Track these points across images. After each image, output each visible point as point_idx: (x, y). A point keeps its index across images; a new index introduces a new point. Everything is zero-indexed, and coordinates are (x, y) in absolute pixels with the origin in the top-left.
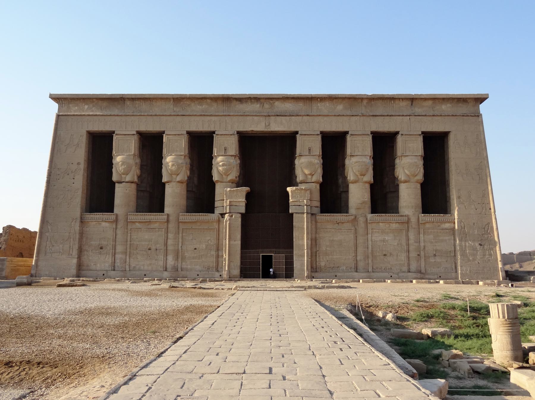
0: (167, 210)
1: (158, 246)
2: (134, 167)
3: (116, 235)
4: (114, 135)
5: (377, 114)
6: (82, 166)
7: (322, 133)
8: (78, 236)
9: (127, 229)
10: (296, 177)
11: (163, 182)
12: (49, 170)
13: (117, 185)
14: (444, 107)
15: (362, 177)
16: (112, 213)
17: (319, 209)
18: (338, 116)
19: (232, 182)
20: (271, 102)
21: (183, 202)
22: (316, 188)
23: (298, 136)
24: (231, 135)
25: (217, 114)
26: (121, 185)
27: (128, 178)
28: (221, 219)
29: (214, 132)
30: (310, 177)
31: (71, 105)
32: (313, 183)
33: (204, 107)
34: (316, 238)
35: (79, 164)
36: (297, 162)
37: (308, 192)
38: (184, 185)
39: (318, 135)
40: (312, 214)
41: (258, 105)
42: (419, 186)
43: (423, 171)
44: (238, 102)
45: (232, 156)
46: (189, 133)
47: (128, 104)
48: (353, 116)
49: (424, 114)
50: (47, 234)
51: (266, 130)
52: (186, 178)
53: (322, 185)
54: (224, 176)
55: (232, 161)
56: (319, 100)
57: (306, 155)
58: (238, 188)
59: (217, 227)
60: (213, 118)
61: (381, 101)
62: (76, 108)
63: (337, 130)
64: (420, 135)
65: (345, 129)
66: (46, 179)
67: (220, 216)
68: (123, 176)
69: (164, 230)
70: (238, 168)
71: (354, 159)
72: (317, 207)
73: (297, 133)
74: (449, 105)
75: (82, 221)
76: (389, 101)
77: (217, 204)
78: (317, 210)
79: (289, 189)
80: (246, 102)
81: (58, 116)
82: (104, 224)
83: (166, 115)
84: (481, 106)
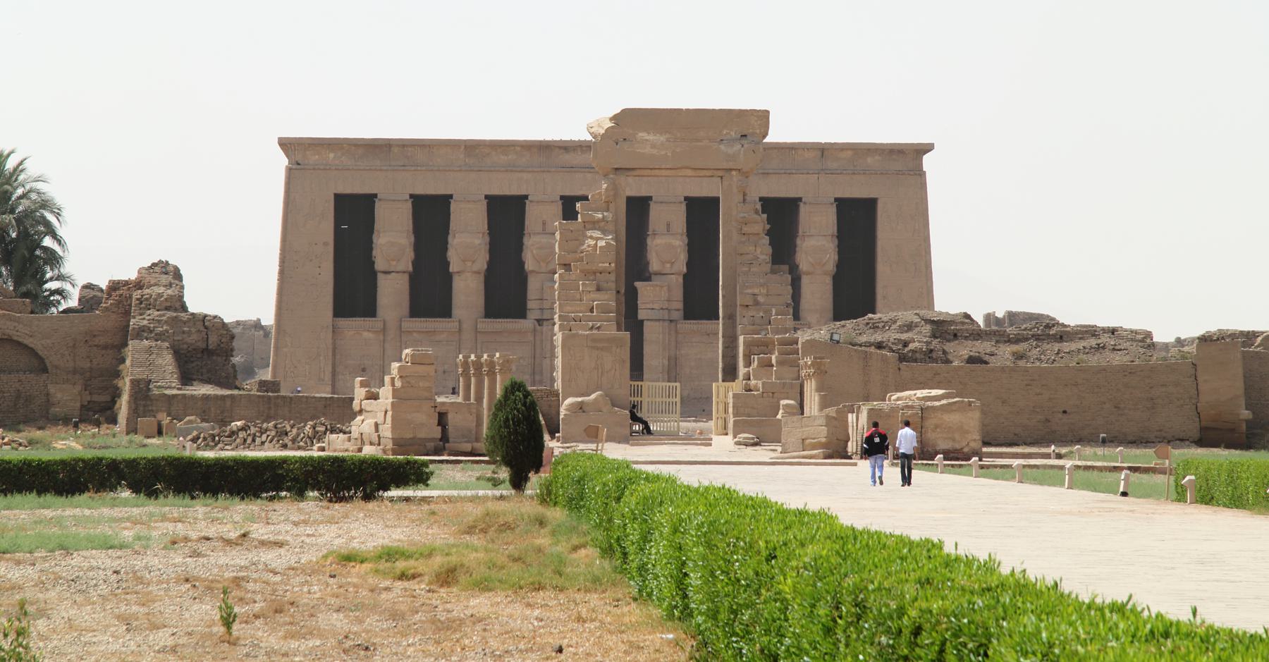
0: (456, 312)
1: (446, 367)
2: (408, 250)
3: (384, 351)
4: (376, 200)
5: (771, 171)
6: (331, 249)
7: (686, 198)
8: (330, 354)
9: (401, 341)
11: (451, 270)
12: (281, 254)
13: (380, 277)
14: (869, 160)
16: (374, 319)
17: (681, 313)
21: (479, 300)
23: (652, 204)
25: (530, 169)
26: (389, 276)
27: (400, 268)
28: (538, 328)
29: (526, 197)
30: (668, 265)
31: (308, 153)
33: (510, 157)
34: (676, 355)
35: (326, 244)
36: (649, 241)
37: (665, 288)
38: (482, 278)
39: (681, 203)
40: (671, 321)
42: (829, 280)
43: (837, 257)
44: (562, 151)
46: (487, 197)
47: (396, 151)
49: (839, 172)
50: (285, 350)
53: (685, 276)
54: (542, 264)
59: (532, 339)
60: (525, 176)
61: (776, 151)
62: (317, 157)
63: (710, 195)
64: (832, 204)
66: (278, 268)
67: (536, 322)
68: (394, 263)
69: (455, 343)
72: (678, 310)
73: (650, 198)
74: (877, 157)
75: (335, 330)
76: (787, 151)
77: (530, 305)
78: (678, 315)
79: (637, 284)
80: (574, 150)
81: (289, 171)
82: (366, 334)
83: (453, 171)
84: (927, 159)
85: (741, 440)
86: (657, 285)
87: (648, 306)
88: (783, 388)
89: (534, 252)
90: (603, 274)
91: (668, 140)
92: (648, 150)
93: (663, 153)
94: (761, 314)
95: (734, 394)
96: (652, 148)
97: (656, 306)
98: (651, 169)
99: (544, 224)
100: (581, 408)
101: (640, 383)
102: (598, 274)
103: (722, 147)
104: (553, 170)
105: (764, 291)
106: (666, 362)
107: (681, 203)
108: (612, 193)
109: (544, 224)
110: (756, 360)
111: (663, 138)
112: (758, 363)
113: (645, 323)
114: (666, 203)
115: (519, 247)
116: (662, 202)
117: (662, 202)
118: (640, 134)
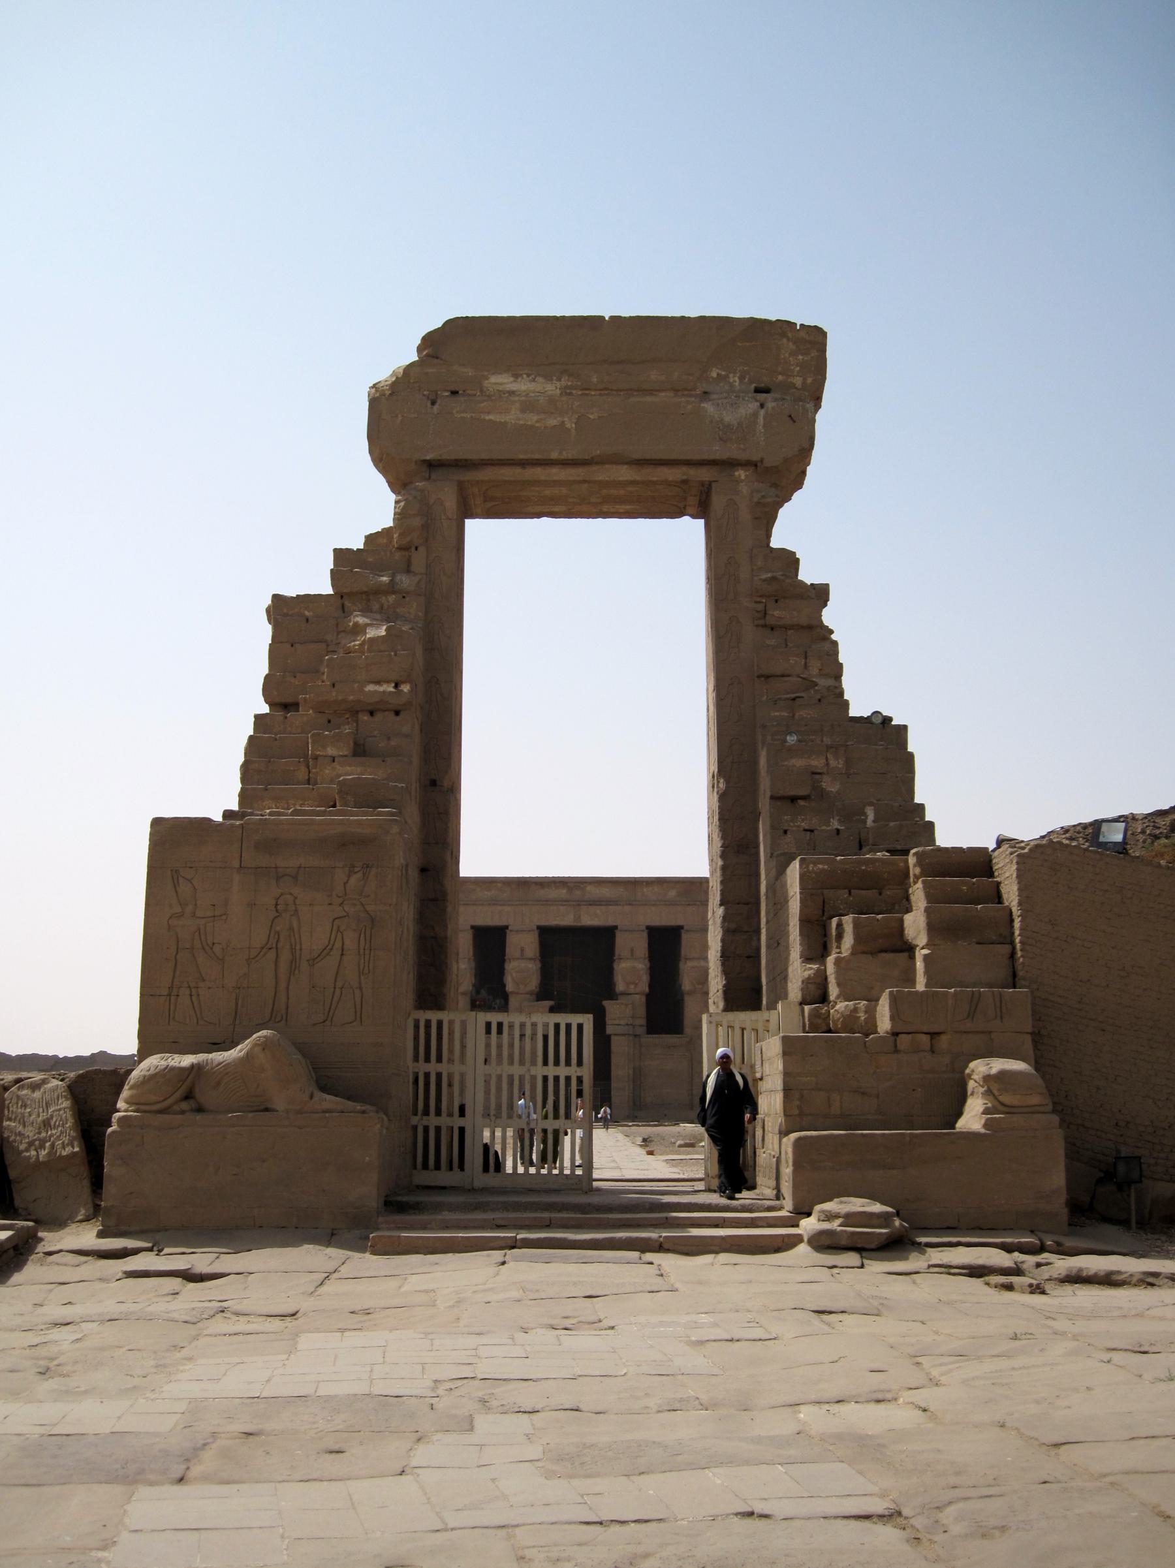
7: (648, 928)
10: (615, 985)
15: (701, 986)
17: (645, 1028)
18: (669, 905)
19: (531, 993)
20: (582, 886)
22: (640, 1000)
24: (529, 931)
30: (632, 986)
32: (636, 994)
33: (493, 892)
36: (615, 966)
37: (630, 1006)
39: (643, 931)
40: (635, 1036)
41: (565, 891)
45: (530, 959)
46: (473, 927)
48: (689, 905)
51: (575, 924)
52: (471, 988)
55: (530, 966)
56: (644, 884)
57: (627, 959)
58: (539, 1002)
60: (506, 908)
65: (679, 923)
70: (539, 971)
71: (690, 964)
72: (641, 1026)
73: (616, 927)
78: (641, 1031)
79: (606, 1003)
85: (835, 1225)
86: (622, 1004)
87: (615, 1022)
88: (971, 1015)
89: (514, 975)
90: (379, 716)
91: (566, 392)
92: (513, 416)
93: (553, 422)
94: (835, 824)
95: (785, 1040)
96: (523, 411)
97: (622, 1022)
98: (523, 464)
99: (522, 950)
100: (188, 1096)
101: (440, 1015)
102: (365, 717)
103: (709, 407)
104: (530, 903)
105: (837, 763)
106: (631, 1072)
107: (643, 931)
108: (417, 522)
109: (522, 950)
110: (849, 928)
111: (552, 388)
112: (858, 938)
113: (614, 1039)
114: (629, 931)
115: (501, 972)
116: (626, 931)
117: (626, 931)
118: (494, 379)
